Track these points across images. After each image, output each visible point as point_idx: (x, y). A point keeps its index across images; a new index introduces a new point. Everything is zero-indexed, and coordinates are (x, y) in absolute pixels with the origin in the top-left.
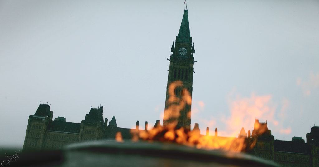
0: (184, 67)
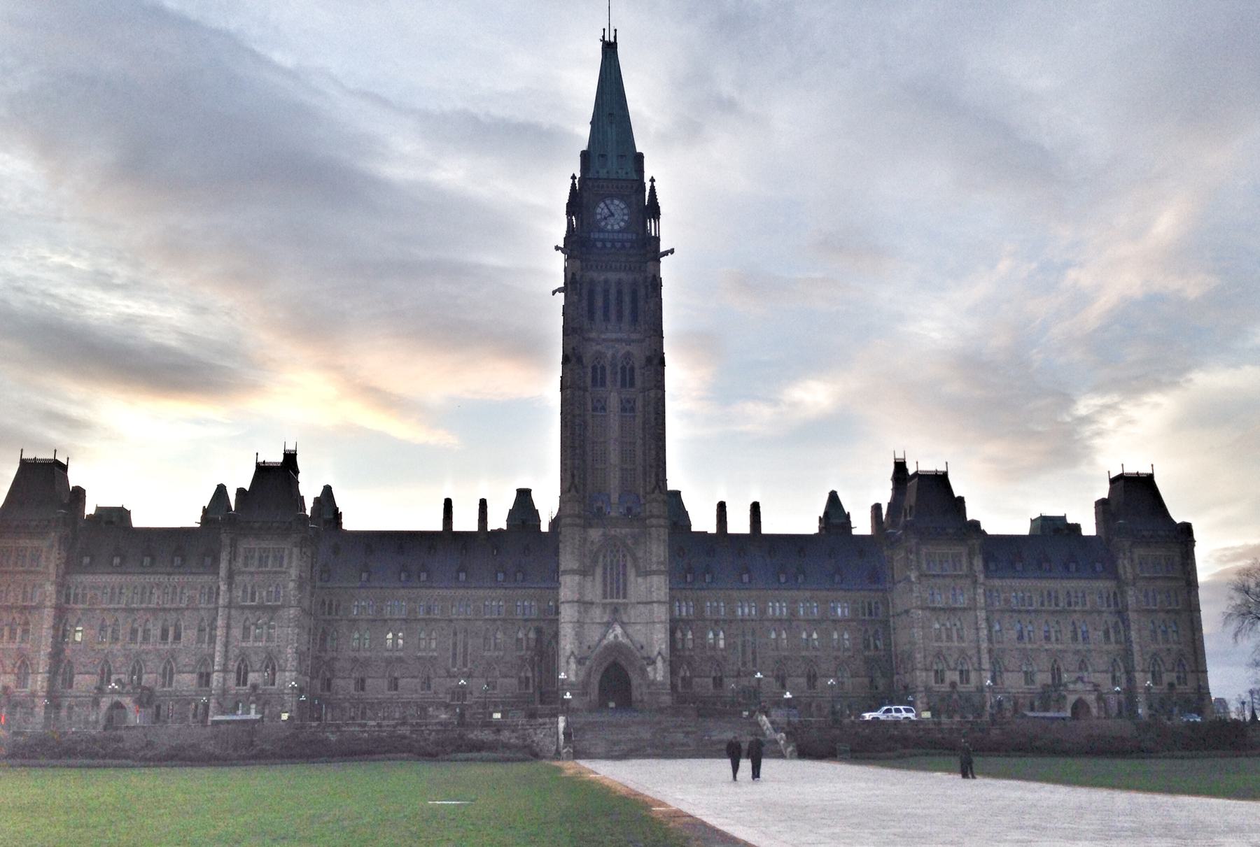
0: (623, 276)
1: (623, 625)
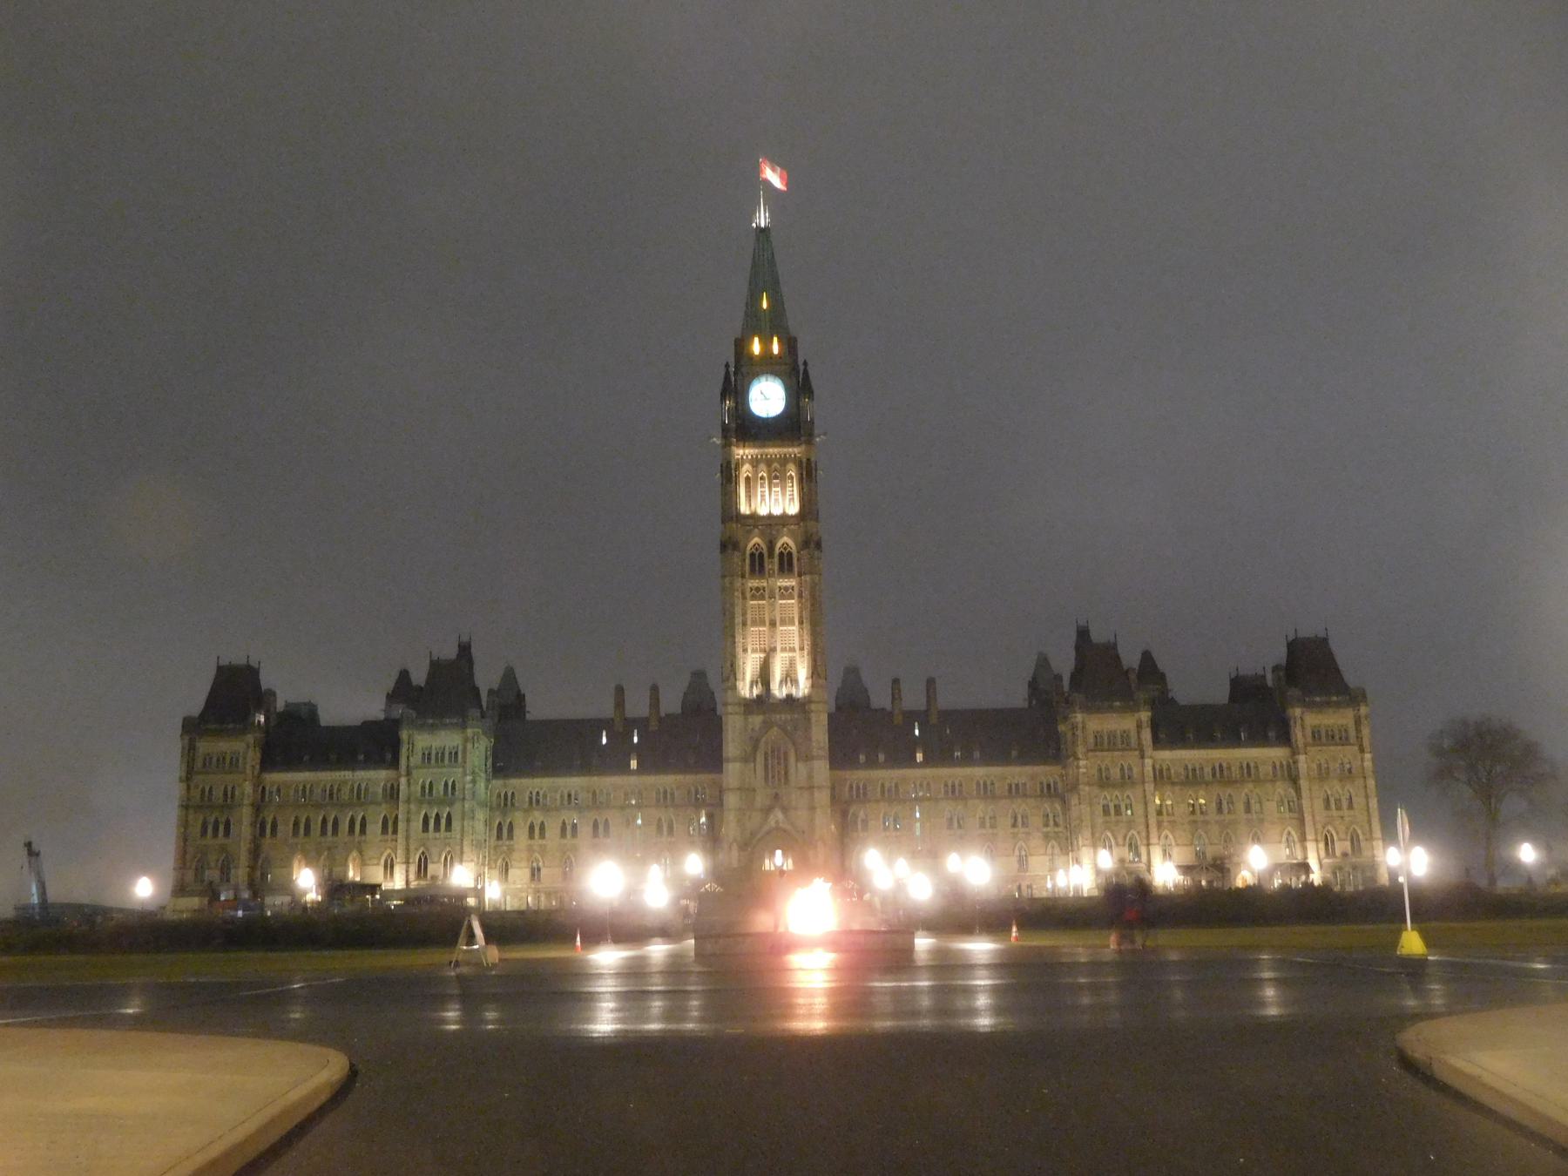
1: (785, 810)
